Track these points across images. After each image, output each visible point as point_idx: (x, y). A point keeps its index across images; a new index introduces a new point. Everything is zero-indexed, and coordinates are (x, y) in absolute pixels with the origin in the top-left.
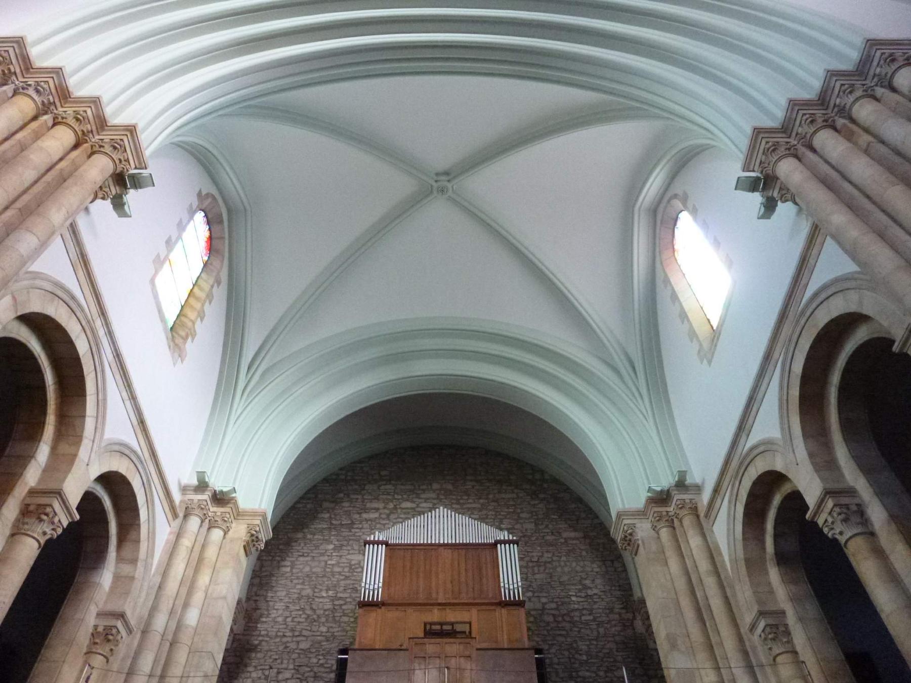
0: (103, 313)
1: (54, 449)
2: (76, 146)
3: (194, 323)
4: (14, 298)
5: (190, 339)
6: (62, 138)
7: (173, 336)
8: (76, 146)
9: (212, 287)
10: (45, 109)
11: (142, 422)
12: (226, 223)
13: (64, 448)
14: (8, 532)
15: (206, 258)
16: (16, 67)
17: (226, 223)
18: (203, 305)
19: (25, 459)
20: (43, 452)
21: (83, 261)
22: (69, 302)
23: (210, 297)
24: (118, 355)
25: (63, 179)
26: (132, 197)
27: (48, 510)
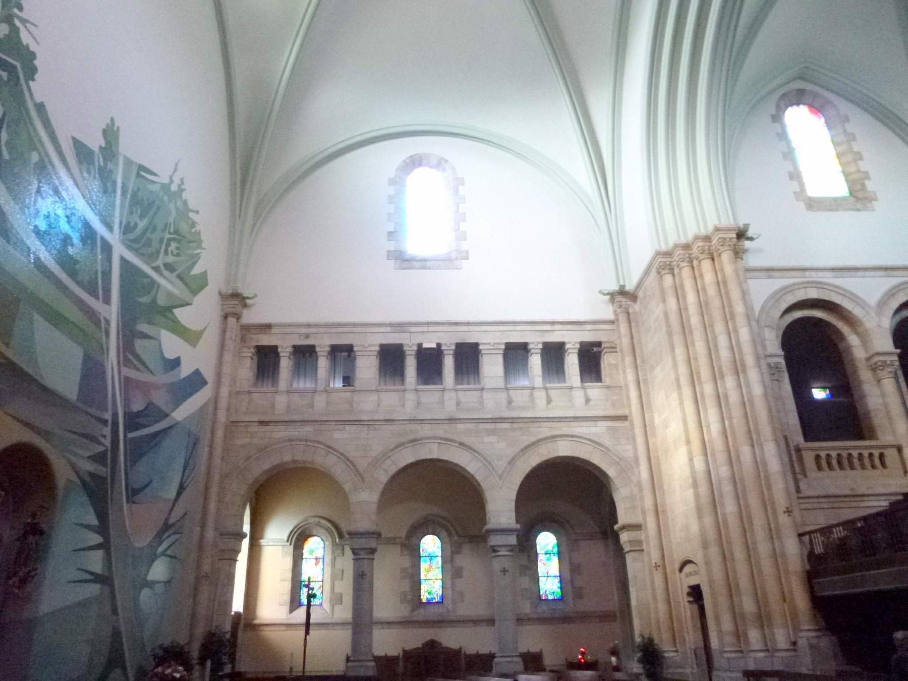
0: (804, 270)
1: (857, 333)
2: (713, 259)
3: (859, 171)
4: (767, 326)
5: (867, 182)
6: (706, 265)
7: (855, 197)
8: (713, 259)
9: (845, 131)
10: (691, 261)
11: (886, 269)
12: (809, 87)
13: (860, 330)
14: (875, 383)
15: (823, 120)
16: (668, 260)
17: (809, 87)
18: (852, 152)
19: (848, 348)
20: (853, 340)
21: (770, 271)
22: (786, 290)
23: (851, 138)
24: (833, 269)
25: (725, 282)
26: (750, 233)
27: (879, 363)
